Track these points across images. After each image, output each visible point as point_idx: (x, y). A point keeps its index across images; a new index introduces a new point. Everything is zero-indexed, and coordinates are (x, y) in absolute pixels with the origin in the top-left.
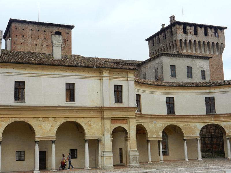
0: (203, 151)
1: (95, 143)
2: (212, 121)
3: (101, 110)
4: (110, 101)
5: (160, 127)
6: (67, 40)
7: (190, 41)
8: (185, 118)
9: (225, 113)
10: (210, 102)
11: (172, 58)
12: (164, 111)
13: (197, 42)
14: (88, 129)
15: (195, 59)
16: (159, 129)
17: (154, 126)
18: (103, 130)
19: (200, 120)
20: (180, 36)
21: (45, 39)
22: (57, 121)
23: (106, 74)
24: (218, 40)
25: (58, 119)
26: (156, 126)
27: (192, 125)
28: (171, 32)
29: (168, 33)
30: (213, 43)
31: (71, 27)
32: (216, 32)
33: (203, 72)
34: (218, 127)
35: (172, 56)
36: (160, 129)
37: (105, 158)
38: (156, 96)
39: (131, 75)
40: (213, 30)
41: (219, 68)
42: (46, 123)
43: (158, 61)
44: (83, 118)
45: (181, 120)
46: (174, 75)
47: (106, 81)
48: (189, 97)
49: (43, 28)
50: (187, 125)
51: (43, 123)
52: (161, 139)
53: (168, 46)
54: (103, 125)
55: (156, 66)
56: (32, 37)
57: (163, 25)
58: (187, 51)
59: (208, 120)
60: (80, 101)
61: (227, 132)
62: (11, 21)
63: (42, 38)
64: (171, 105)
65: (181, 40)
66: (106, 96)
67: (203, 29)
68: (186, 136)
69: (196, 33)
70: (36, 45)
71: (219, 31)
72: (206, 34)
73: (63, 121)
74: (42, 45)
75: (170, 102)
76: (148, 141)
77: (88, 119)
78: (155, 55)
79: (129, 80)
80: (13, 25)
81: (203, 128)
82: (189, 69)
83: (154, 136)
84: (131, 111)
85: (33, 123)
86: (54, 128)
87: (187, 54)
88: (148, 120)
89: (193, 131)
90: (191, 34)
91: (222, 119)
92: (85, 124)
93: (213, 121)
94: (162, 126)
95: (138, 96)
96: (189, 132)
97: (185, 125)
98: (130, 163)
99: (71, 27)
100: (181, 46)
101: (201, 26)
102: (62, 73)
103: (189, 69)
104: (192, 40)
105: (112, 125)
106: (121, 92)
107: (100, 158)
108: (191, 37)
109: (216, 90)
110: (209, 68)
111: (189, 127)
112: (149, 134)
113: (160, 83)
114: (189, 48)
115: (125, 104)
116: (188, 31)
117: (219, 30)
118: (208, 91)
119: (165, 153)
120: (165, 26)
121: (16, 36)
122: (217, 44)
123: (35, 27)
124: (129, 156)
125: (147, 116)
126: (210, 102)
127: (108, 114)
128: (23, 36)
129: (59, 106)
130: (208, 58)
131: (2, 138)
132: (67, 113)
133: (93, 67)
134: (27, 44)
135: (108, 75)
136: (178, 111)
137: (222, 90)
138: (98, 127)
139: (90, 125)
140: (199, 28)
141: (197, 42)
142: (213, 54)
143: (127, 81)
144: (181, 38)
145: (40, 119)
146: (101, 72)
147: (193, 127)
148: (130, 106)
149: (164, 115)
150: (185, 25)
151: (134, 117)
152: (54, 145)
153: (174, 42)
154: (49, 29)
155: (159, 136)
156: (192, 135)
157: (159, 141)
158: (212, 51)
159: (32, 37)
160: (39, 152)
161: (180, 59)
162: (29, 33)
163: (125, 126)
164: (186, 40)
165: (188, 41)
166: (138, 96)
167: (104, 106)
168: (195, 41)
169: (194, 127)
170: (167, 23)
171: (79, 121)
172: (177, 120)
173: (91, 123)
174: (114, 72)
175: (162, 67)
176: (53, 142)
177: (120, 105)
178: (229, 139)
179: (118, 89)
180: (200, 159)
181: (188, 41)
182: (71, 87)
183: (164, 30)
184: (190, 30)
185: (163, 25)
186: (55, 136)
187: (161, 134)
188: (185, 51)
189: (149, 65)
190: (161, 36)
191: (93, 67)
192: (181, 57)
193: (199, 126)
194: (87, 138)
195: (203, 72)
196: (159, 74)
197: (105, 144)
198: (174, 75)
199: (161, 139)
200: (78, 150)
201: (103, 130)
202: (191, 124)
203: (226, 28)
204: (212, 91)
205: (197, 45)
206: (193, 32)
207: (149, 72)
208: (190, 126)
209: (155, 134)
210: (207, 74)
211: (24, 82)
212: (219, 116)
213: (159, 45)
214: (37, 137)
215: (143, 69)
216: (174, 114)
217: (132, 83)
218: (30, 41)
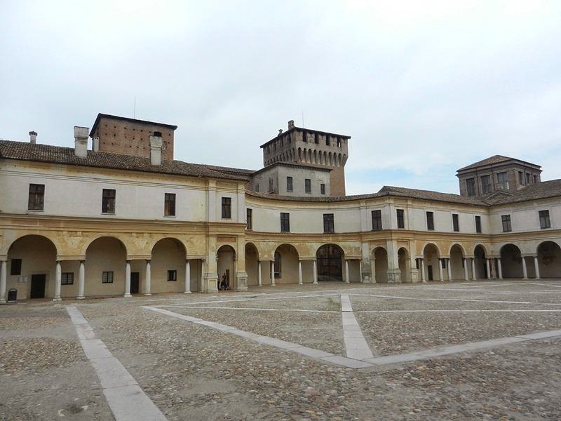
0: (319, 273)
1: (198, 264)
2: (330, 241)
3: (205, 226)
4: (216, 215)
9: (345, 232)
10: (329, 220)
12: (278, 229)
13: (318, 152)
18: (207, 250)
19: (318, 239)
20: (299, 144)
23: (212, 184)
27: (308, 244)
28: (290, 139)
29: (285, 140)
30: (335, 154)
31: (175, 128)
32: (338, 141)
33: (323, 186)
34: (336, 247)
37: (209, 280)
38: (269, 211)
39: (241, 187)
40: (336, 140)
41: (340, 182)
42: (140, 239)
43: (273, 171)
45: (296, 239)
46: (290, 188)
47: (212, 193)
48: (306, 213)
49: (140, 127)
52: (274, 260)
53: (285, 154)
54: (207, 243)
55: (271, 177)
57: (281, 131)
58: (306, 162)
60: (182, 214)
61: (346, 253)
62: (101, 116)
63: (138, 138)
64: (286, 222)
65: (300, 148)
66: (212, 210)
67: (325, 138)
68: (302, 257)
69: (317, 142)
71: (342, 140)
72: (328, 143)
73: (160, 237)
75: (285, 219)
76: (259, 262)
77: (190, 236)
78: (270, 164)
80: (103, 121)
81: (320, 248)
82: (308, 182)
83: (266, 256)
84: (240, 227)
85: (124, 239)
87: (306, 165)
88: (260, 238)
91: (341, 238)
95: (249, 211)
98: (237, 286)
99: (175, 128)
100: (300, 156)
101: (322, 134)
102: (161, 182)
103: (308, 182)
106: (230, 205)
107: (203, 281)
108: (311, 146)
109: (336, 207)
110: (329, 182)
112: (260, 254)
113: (274, 196)
114: (309, 158)
115: (233, 220)
116: (308, 139)
117: (342, 139)
118: (327, 207)
119: (277, 276)
120: (283, 132)
122: (340, 154)
123: (129, 125)
124: (237, 278)
125: (257, 234)
126: (329, 220)
127: (213, 230)
129: (156, 220)
130: (328, 170)
132: (164, 228)
133: (197, 176)
136: (294, 229)
137: (341, 206)
138: (201, 245)
139: (192, 243)
140: (320, 137)
141: (318, 152)
145: (133, 234)
146: (207, 182)
148: (240, 222)
150: (305, 131)
151: (243, 234)
152: (149, 266)
153: (292, 151)
154: (146, 128)
157: (271, 261)
158: (334, 163)
160: (131, 273)
162: (123, 131)
163: (232, 245)
165: (307, 150)
166: (249, 211)
167: (210, 221)
168: (315, 151)
169: (310, 246)
170: (285, 129)
171: (180, 238)
172: (292, 239)
173: (194, 240)
175: (278, 179)
176: (148, 261)
177: (228, 221)
178: (347, 260)
179: (226, 203)
180: (316, 282)
181: (307, 150)
182: (172, 197)
183: (281, 136)
184: (310, 138)
185: (281, 131)
187: (273, 254)
189: (263, 176)
190: (278, 143)
191: (197, 176)
193: (316, 246)
194: (188, 258)
195: (323, 186)
196: (274, 186)
197: (210, 265)
198: (290, 188)
199: (274, 260)
200: (178, 272)
201: (207, 250)
202: (309, 244)
203: (350, 138)
204: (331, 207)
205: (318, 155)
206: (313, 140)
207: (263, 182)
210: (327, 188)
211: (114, 191)
212: (338, 235)
213: (275, 153)
215: (256, 179)
217: (242, 195)
218: (124, 142)
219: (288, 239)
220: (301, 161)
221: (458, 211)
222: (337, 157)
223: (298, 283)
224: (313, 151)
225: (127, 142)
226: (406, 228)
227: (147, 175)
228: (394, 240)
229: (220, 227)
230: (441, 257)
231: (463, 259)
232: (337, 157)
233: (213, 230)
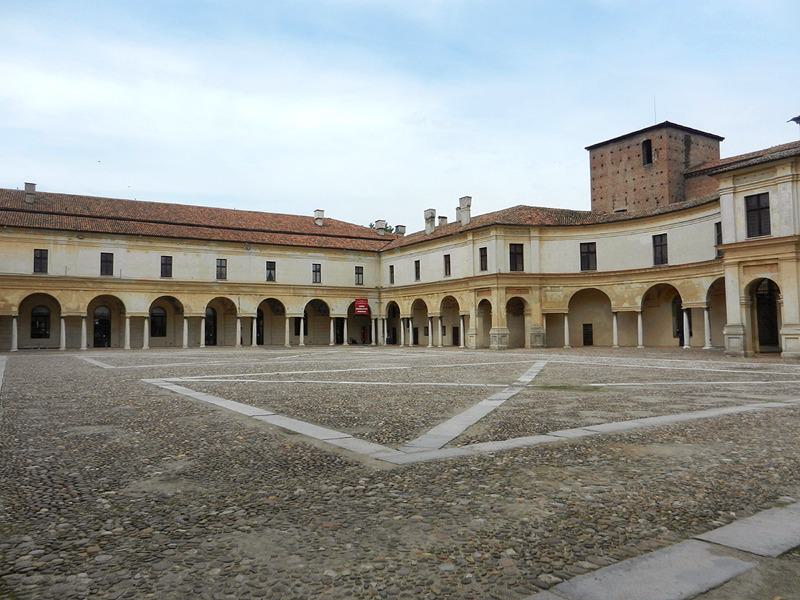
8: (680, 270)
12: (649, 262)
19: (708, 270)
38: (632, 238)
49: (626, 143)
63: (625, 158)
64: (659, 248)
81: (712, 286)
83: (626, 305)
88: (613, 279)
112: (613, 303)
115: (492, 269)
123: (614, 147)
125: (607, 275)
173: (464, 297)
177: (485, 273)
187: (639, 301)
218: (611, 169)
219: (665, 275)
225: (615, 169)
228: (729, 264)
229: (476, 280)
233: (473, 285)
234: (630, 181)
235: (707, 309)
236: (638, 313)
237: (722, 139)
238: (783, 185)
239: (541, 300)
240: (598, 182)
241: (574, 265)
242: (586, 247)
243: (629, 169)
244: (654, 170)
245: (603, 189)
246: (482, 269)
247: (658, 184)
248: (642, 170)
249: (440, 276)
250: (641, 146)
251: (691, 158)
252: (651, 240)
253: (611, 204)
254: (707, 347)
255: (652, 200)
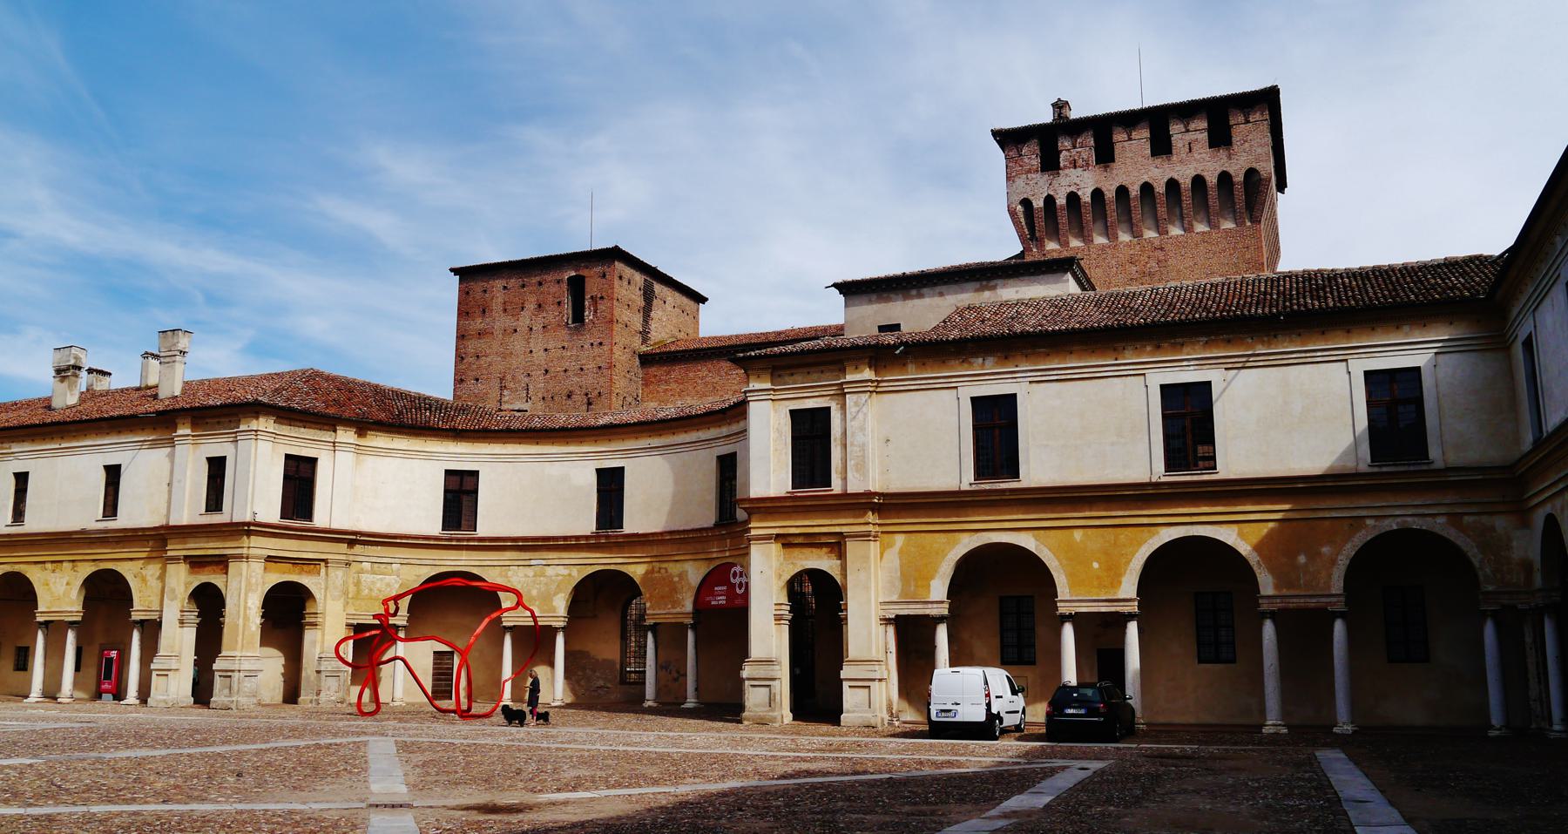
1: (152, 629)
5: (560, 578)
6: (602, 298)
7: (1073, 198)
11: (885, 295)
14: (140, 592)
15: (992, 283)
16: (553, 587)
17: (534, 576)
21: (540, 306)
22: (79, 570)
24: (1229, 157)
25: (79, 564)
26: (541, 576)
27: (674, 569)
35: (884, 291)
36: (558, 586)
38: (555, 470)
44: (131, 559)
50: (659, 572)
51: (52, 574)
56: (505, 310)
58: (1066, 244)
59: (717, 548)
63: (531, 306)
67: (1143, 135)
69: (1105, 156)
70: (516, 331)
74: (531, 329)
79: (239, 438)
86: (71, 589)
89: (676, 593)
90: (1075, 167)
92: (135, 577)
93: (727, 554)
94: (570, 575)
96: (663, 597)
97: (653, 568)
104: (1079, 193)
105: (191, 578)
111: (664, 579)
116: (1063, 158)
121: (468, 313)
128: (484, 311)
129: (83, 532)
131: (84, 613)
134: (492, 333)
135: (188, 431)
139: (144, 580)
142: (1207, 229)
143: (234, 443)
144: (1025, 196)
147: (676, 579)
149: (571, 537)
155: (554, 612)
156: (673, 607)
159: (505, 310)
161: (920, 296)
163: (217, 580)
164: (1050, 200)
165: (1061, 201)
171: (121, 568)
174: (208, 421)
186: (80, 608)
187: (561, 605)
188: (1051, 246)
192: (925, 286)
208: (667, 572)
209: (537, 603)
214: (39, 613)
216: (618, 532)
218: (501, 321)
220: (1041, 245)
221: (1202, 362)
222: (1213, 194)
223: (56, 699)
224: (1086, 197)
226: (836, 487)
227: (76, 431)
230: (1063, 609)
231: (498, 631)
232: (1213, 194)
234: (539, 355)
235: (694, 627)
236: (556, 630)
237: (702, 300)
238: (855, 397)
239: (346, 593)
240: (472, 346)
241: (428, 519)
242: (457, 478)
243: (537, 327)
244: (587, 339)
245: (483, 361)
246: (208, 509)
247: (591, 365)
248: (563, 333)
249: (88, 516)
250: (565, 286)
251: (653, 325)
252: (593, 479)
253: (495, 393)
254: (691, 703)
255: (579, 398)
